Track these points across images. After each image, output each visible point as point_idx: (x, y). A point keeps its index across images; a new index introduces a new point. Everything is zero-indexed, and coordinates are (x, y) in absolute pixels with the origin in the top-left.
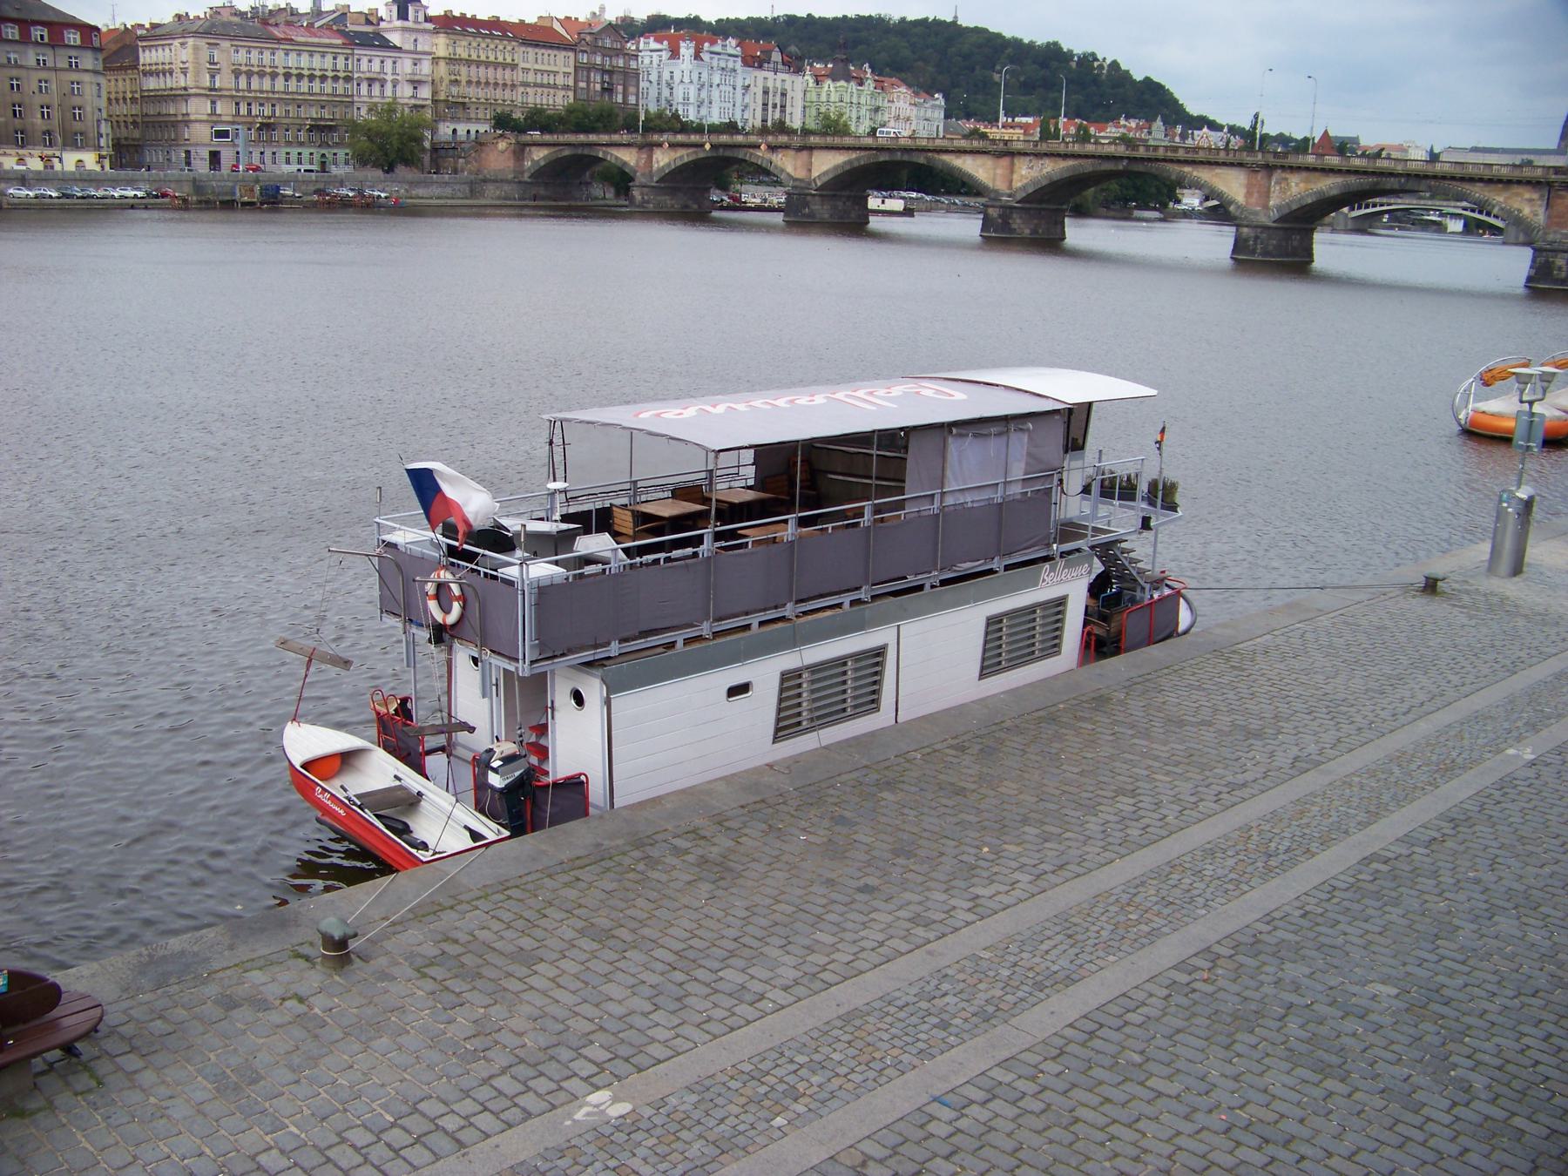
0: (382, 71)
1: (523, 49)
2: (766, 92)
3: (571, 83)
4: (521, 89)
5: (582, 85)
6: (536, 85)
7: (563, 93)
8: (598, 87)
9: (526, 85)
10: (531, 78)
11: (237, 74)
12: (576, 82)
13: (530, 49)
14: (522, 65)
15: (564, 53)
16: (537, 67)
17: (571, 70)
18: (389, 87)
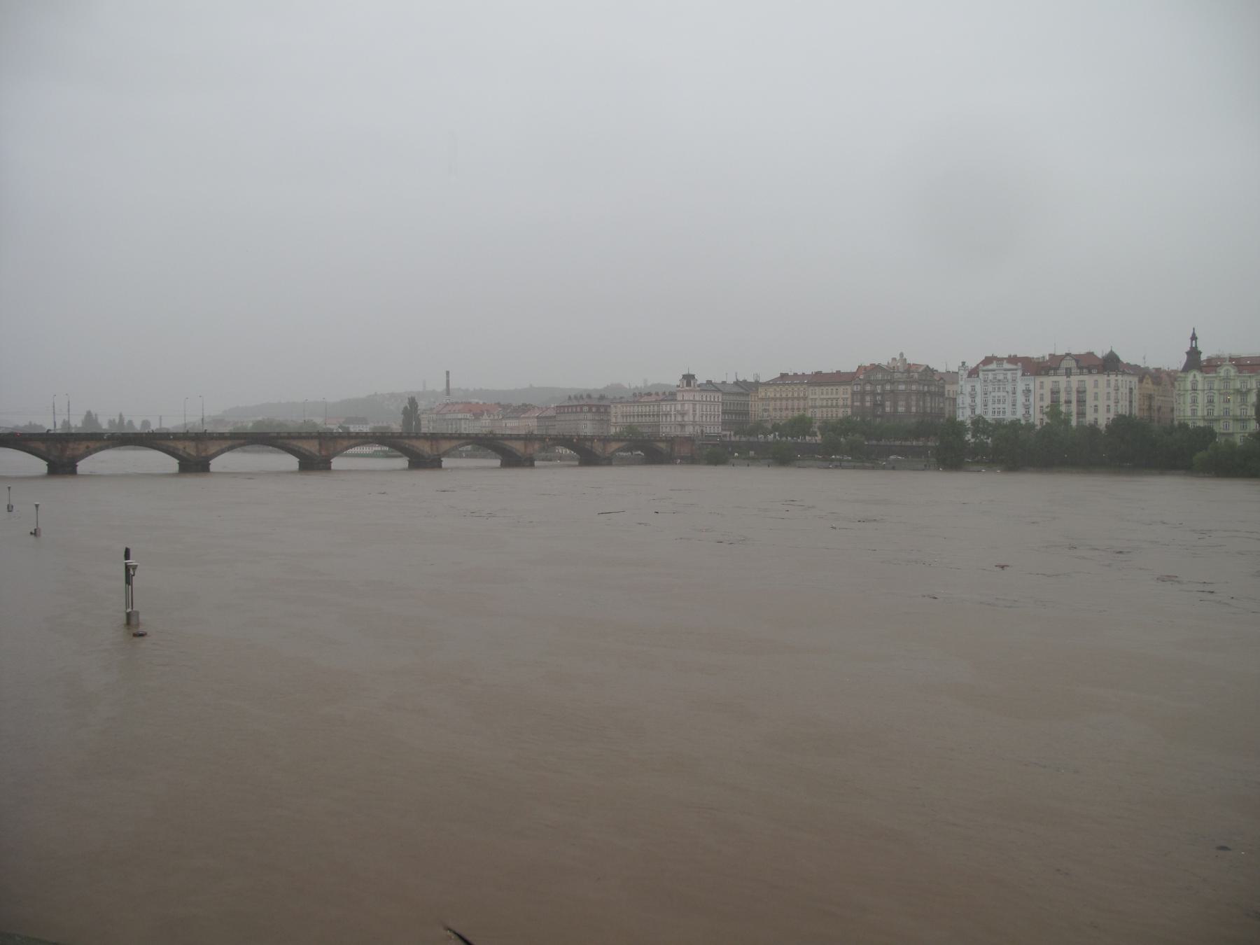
0: (671, 411)
1: (811, 388)
2: (1055, 392)
3: (849, 403)
4: (811, 410)
5: (858, 404)
6: (822, 407)
7: (843, 410)
8: (868, 404)
9: (815, 407)
10: (818, 403)
11: (623, 416)
12: (853, 402)
13: (816, 388)
14: (811, 397)
15: (843, 387)
16: (822, 397)
17: (849, 396)
18: (673, 418)
